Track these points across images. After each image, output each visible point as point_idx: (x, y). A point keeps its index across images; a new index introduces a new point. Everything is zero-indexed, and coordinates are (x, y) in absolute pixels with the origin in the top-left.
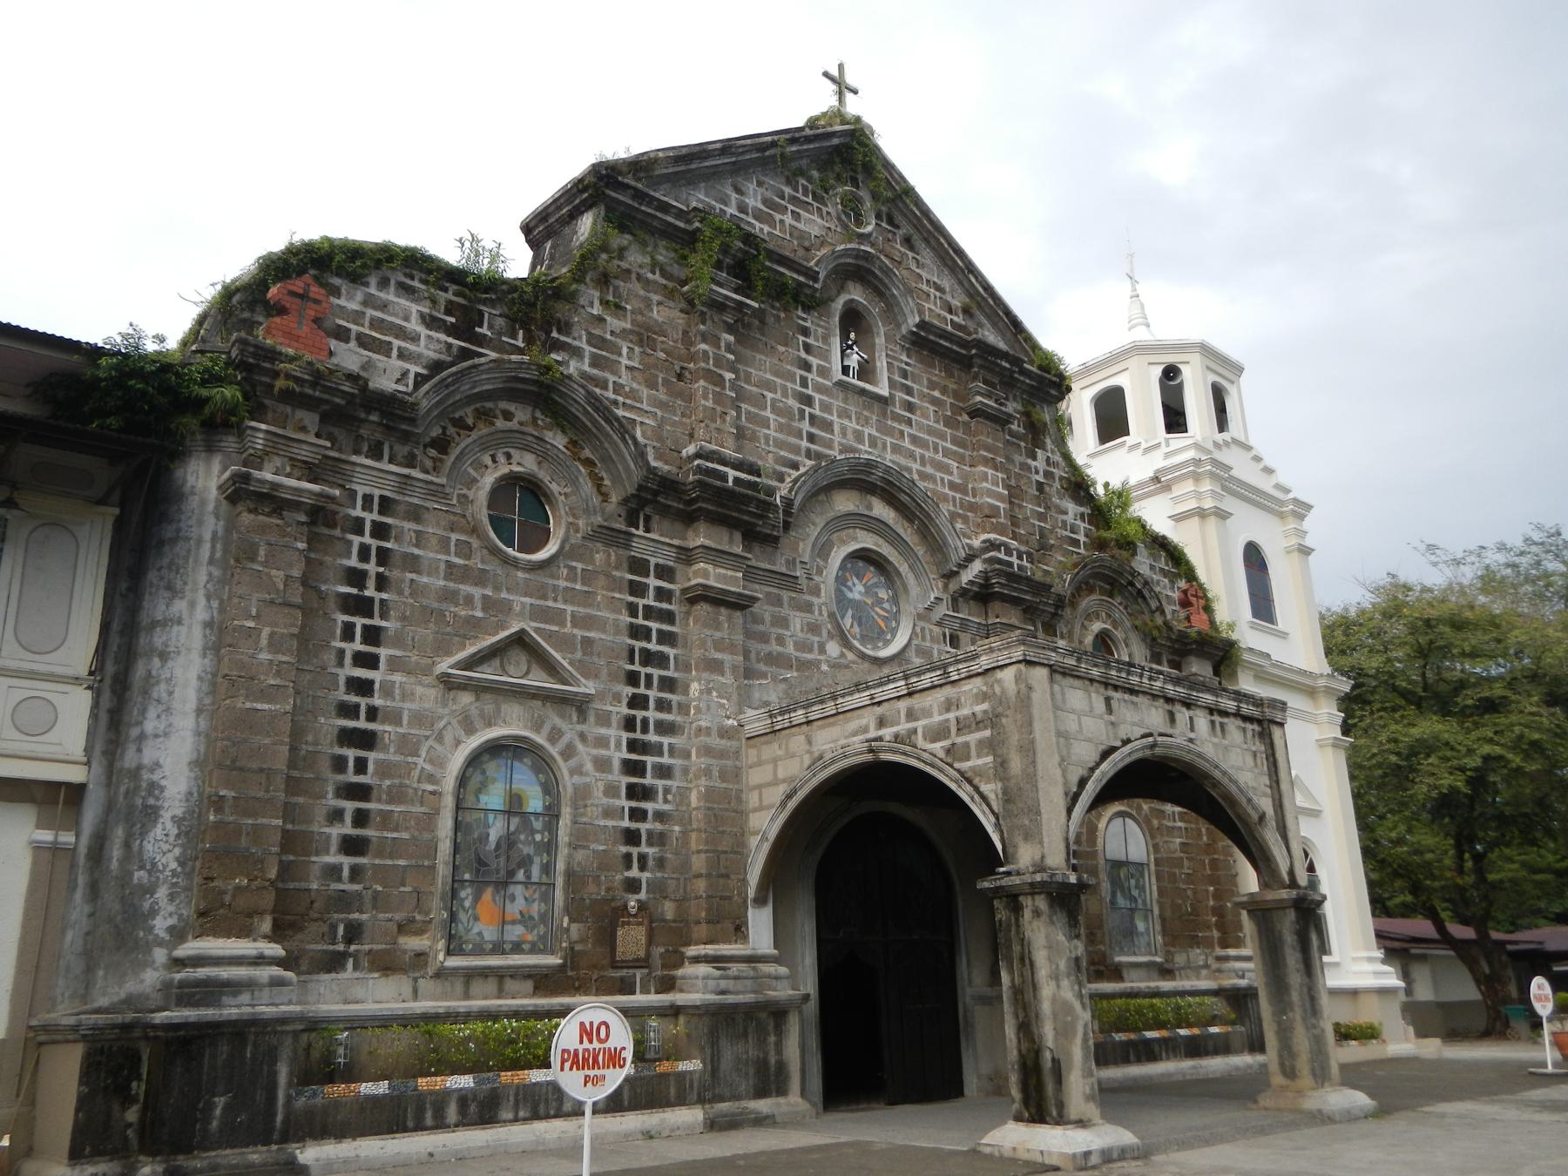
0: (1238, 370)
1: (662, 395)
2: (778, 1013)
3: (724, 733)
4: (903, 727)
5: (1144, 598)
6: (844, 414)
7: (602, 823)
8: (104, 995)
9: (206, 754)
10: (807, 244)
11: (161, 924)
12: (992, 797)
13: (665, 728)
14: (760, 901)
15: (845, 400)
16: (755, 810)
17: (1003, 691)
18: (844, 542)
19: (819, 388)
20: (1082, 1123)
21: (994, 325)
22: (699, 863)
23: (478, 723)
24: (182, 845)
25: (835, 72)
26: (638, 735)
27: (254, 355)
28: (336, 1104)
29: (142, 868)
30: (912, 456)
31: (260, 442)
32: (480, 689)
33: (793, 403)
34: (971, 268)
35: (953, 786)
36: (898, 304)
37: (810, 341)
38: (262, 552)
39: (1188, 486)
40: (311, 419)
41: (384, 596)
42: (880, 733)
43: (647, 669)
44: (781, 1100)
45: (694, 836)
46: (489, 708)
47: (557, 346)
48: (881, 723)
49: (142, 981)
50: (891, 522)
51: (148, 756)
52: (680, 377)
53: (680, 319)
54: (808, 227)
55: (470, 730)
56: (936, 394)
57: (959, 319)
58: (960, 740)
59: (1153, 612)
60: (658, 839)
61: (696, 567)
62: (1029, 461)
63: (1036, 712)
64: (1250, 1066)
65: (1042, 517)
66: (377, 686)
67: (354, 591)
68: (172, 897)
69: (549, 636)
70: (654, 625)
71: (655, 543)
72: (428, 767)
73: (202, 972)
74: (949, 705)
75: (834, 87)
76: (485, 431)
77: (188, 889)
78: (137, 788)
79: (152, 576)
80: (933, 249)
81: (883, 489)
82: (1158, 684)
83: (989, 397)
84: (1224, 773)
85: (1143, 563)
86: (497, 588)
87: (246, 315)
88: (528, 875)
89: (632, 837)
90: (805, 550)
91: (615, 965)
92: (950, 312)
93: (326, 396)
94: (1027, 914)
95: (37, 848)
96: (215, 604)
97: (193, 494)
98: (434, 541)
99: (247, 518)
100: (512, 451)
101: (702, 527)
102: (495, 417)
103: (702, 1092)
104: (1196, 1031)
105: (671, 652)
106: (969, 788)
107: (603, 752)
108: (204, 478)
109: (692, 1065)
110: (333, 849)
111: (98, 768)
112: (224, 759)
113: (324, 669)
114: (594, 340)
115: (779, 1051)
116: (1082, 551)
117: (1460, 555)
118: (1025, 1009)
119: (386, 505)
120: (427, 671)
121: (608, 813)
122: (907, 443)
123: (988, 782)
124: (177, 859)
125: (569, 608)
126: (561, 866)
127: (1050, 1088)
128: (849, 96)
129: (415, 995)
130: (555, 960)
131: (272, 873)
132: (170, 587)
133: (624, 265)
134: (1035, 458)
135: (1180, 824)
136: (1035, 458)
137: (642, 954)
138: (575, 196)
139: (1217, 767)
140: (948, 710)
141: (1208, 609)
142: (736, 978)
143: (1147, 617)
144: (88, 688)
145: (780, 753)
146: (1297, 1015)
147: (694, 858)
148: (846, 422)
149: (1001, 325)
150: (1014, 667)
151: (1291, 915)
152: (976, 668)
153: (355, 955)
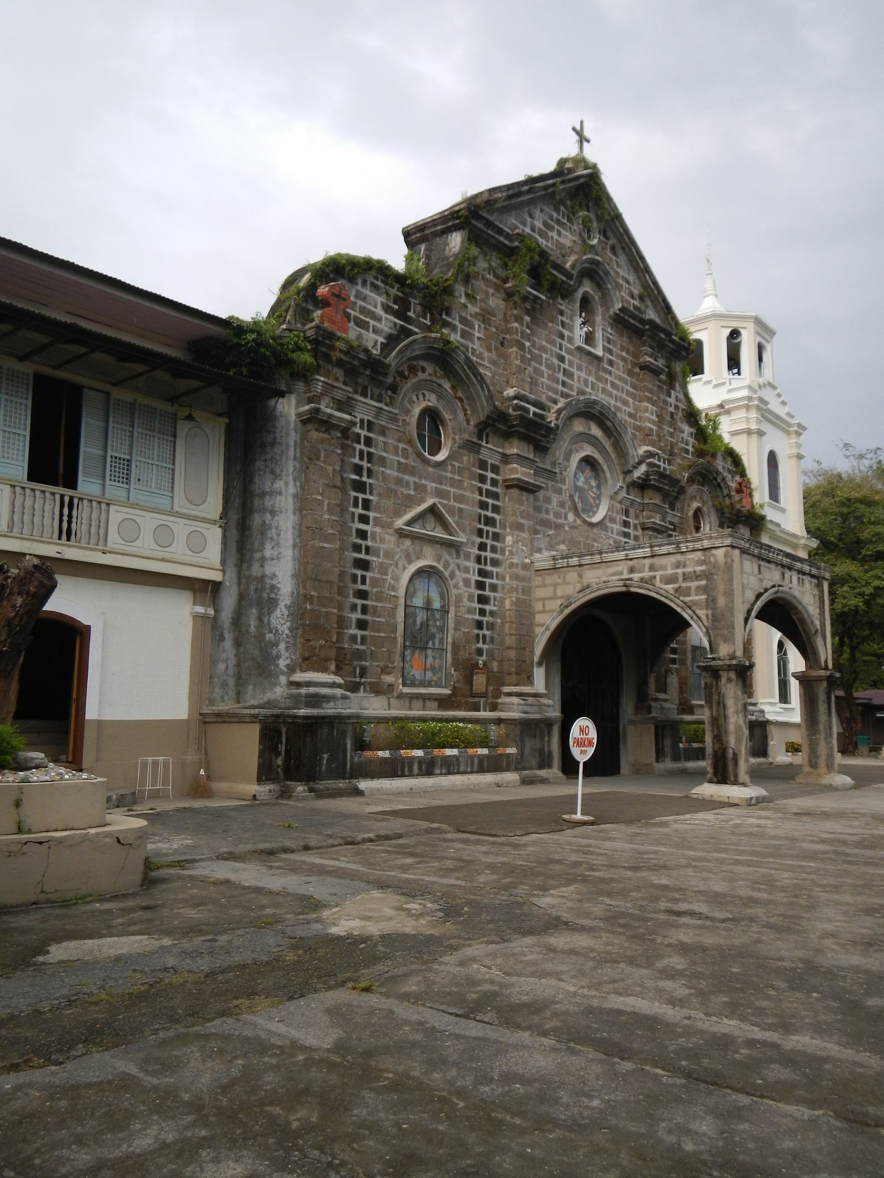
0: (772, 333)
1: (494, 356)
2: (548, 724)
3: (525, 567)
4: (647, 574)
5: (721, 488)
6: (579, 368)
7: (467, 616)
8: (254, 698)
9: (299, 570)
10: (564, 253)
11: (283, 663)
12: (704, 617)
13: (495, 563)
14: (540, 664)
15: (580, 359)
16: (539, 612)
17: (716, 561)
18: (577, 451)
19: (569, 351)
20: (744, 785)
21: (655, 307)
22: (510, 641)
23: (413, 557)
24: (290, 621)
25: (578, 127)
26: (482, 566)
27: (323, 336)
28: (370, 761)
29: (270, 632)
30: (610, 395)
31: (319, 388)
32: (414, 537)
33: (555, 361)
34: (647, 270)
35: (679, 610)
36: (610, 295)
37: (564, 319)
38: (322, 455)
39: (742, 413)
40: (340, 373)
41: (371, 481)
42: (632, 576)
43: (487, 527)
44: (549, 770)
45: (507, 625)
46: (418, 548)
47: (446, 324)
48: (632, 570)
49: (275, 693)
50: (600, 438)
51: (269, 570)
52: (502, 344)
53: (502, 305)
54: (562, 239)
55: (410, 562)
56: (624, 354)
57: (636, 303)
58: (684, 585)
59: (725, 497)
60: (491, 626)
61: (511, 466)
62: (668, 399)
63: (735, 574)
65: (672, 435)
66: (369, 534)
67: (357, 478)
68: (287, 649)
69: (444, 506)
70: (490, 501)
71: (491, 450)
72: (392, 582)
73: (312, 690)
74: (678, 565)
75: (576, 138)
76: (415, 380)
77: (295, 645)
78: (263, 588)
79: (259, 464)
80: (627, 255)
81: (598, 418)
82: (780, 557)
83: (651, 356)
84: (803, 607)
85: (721, 464)
86: (420, 478)
87: (304, 305)
88: (434, 645)
89: (479, 625)
90: (560, 454)
91: (473, 695)
92: (633, 298)
93: (351, 361)
94: (724, 680)
95: (196, 617)
96: (298, 484)
97: (281, 416)
98: (392, 448)
99: (314, 435)
100: (426, 392)
101: (515, 442)
102: (418, 370)
103: (515, 764)
105: (497, 517)
106: (690, 612)
107: (468, 576)
108: (289, 409)
109: (512, 750)
110: (354, 626)
111: (232, 574)
112: (308, 573)
113: (346, 523)
114: (464, 321)
115: (549, 746)
116: (690, 457)
117: (864, 452)
118: (718, 728)
119: (370, 426)
120: (390, 525)
121: (470, 611)
122: (609, 387)
123: (702, 609)
124: (288, 628)
125: (452, 490)
126: (450, 640)
127: (731, 767)
128: (585, 144)
129: (389, 708)
130: (447, 691)
131: (334, 639)
132: (272, 472)
133: (476, 269)
134: (670, 396)
136: (670, 396)
137: (484, 690)
138: (449, 220)
139: (801, 604)
140: (678, 567)
141: (751, 495)
142: (531, 705)
143: (721, 499)
144: (220, 526)
145: (559, 581)
146: (822, 737)
147: (507, 638)
148: (580, 373)
149: (659, 307)
150: (723, 549)
151: (825, 684)
152: (698, 545)
153: (364, 684)
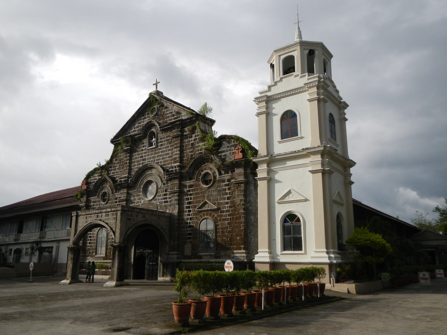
33: (140, 159)
128: (158, 84)
135: (228, 217)
136: (192, 137)
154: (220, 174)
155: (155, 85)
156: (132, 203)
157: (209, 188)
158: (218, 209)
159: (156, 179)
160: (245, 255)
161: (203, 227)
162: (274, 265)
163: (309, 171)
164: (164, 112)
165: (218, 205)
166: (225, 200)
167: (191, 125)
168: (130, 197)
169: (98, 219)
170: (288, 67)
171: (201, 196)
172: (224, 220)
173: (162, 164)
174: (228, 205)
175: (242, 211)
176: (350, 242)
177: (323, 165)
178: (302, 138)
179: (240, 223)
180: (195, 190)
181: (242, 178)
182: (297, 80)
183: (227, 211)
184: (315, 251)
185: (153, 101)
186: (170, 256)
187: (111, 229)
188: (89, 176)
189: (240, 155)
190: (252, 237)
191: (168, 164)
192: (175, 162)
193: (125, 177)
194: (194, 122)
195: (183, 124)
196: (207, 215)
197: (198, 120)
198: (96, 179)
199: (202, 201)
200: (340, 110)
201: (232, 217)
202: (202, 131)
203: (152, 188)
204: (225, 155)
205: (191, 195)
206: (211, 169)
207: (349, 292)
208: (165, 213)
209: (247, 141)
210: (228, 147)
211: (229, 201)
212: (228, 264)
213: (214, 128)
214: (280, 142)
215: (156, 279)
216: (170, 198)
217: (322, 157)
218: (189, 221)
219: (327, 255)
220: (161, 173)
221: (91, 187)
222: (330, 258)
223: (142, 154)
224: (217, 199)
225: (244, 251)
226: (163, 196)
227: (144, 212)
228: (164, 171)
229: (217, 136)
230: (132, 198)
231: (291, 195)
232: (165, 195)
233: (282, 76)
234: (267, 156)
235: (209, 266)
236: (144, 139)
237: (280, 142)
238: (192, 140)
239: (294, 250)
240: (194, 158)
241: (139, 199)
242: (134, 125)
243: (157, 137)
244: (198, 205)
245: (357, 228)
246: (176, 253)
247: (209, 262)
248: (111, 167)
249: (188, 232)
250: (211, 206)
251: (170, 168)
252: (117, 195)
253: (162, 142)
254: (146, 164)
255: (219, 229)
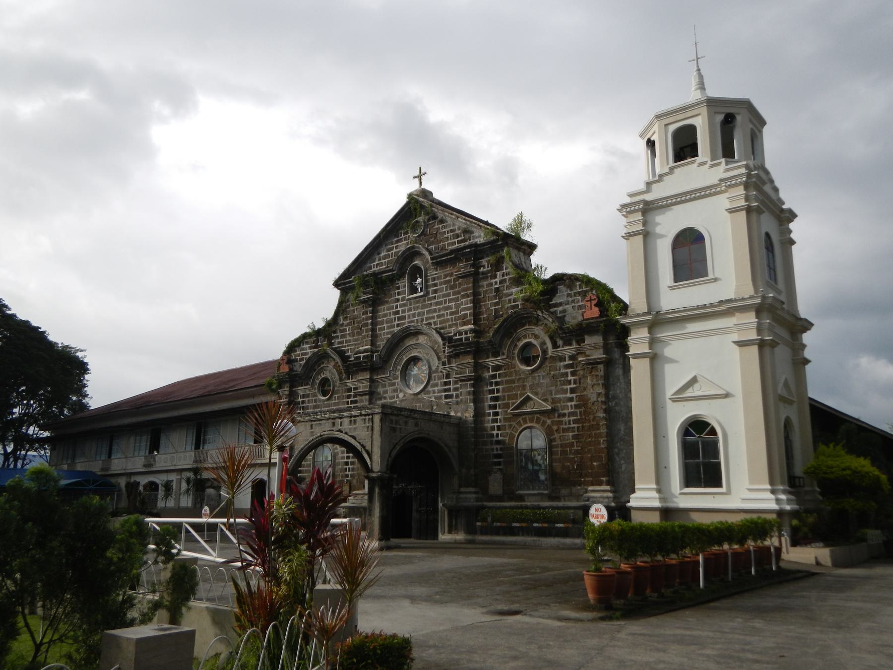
30: (439, 310)
33: (392, 317)
64: (575, 544)
104: (546, 525)
128: (423, 177)
136: (495, 277)
154: (555, 346)
155: (417, 179)
156: (380, 399)
157: (533, 371)
158: (553, 410)
159: (427, 354)
160: (610, 495)
161: (523, 443)
162: (667, 512)
163: (734, 342)
164: (438, 229)
165: (552, 403)
166: (566, 393)
167: (494, 254)
168: (377, 387)
169: (334, 428)
170: (685, 147)
171: (519, 387)
172: (564, 430)
173: (438, 326)
174: (573, 403)
175: (601, 415)
176: (812, 473)
177: (759, 330)
178: (716, 280)
179: (600, 435)
180: (506, 375)
181: (599, 354)
182: (703, 171)
183: (570, 414)
184: (748, 489)
185: (415, 209)
186: (462, 496)
187: (363, 447)
188: (293, 347)
189: (595, 312)
190: (622, 462)
191: (450, 326)
192: (464, 324)
193: (365, 351)
194: (501, 247)
195: (477, 252)
196: (531, 421)
197: (507, 244)
198: (306, 354)
199: (521, 396)
200: (781, 225)
201: (580, 425)
202: (517, 266)
203: (419, 371)
204: (564, 311)
205: (497, 384)
206: (536, 337)
207: (818, 563)
208: (448, 416)
209: (605, 285)
210: (569, 295)
211: (574, 395)
212: (596, 510)
213: (536, 259)
214: (671, 288)
215: (436, 537)
216: (456, 389)
217: (757, 317)
218: (495, 432)
219: (772, 496)
220: (436, 342)
221: (298, 368)
222: (778, 501)
223: (397, 307)
224: (551, 391)
225: (608, 488)
226: (441, 385)
227: (417, 416)
228: (443, 340)
229: (547, 275)
230: (380, 390)
231: (696, 386)
232: (446, 384)
233: (671, 164)
234: (649, 313)
235: (539, 514)
236: (399, 280)
237: (671, 288)
238: (496, 283)
239: (707, 485)
240: (502, 315)
241: (395, 391)
242: (379, 254)
243: (426, 276)
244: (513, 404)
245: (822, 447)
246: (472, 490)
247: (539, 508)
248: (335, 332)
249: (495, 452)
250: (539, 404)
251: (455, 335)
252: (351, 383)
253: (435, 285)
254: (407, 327)
255: (557, 446)
